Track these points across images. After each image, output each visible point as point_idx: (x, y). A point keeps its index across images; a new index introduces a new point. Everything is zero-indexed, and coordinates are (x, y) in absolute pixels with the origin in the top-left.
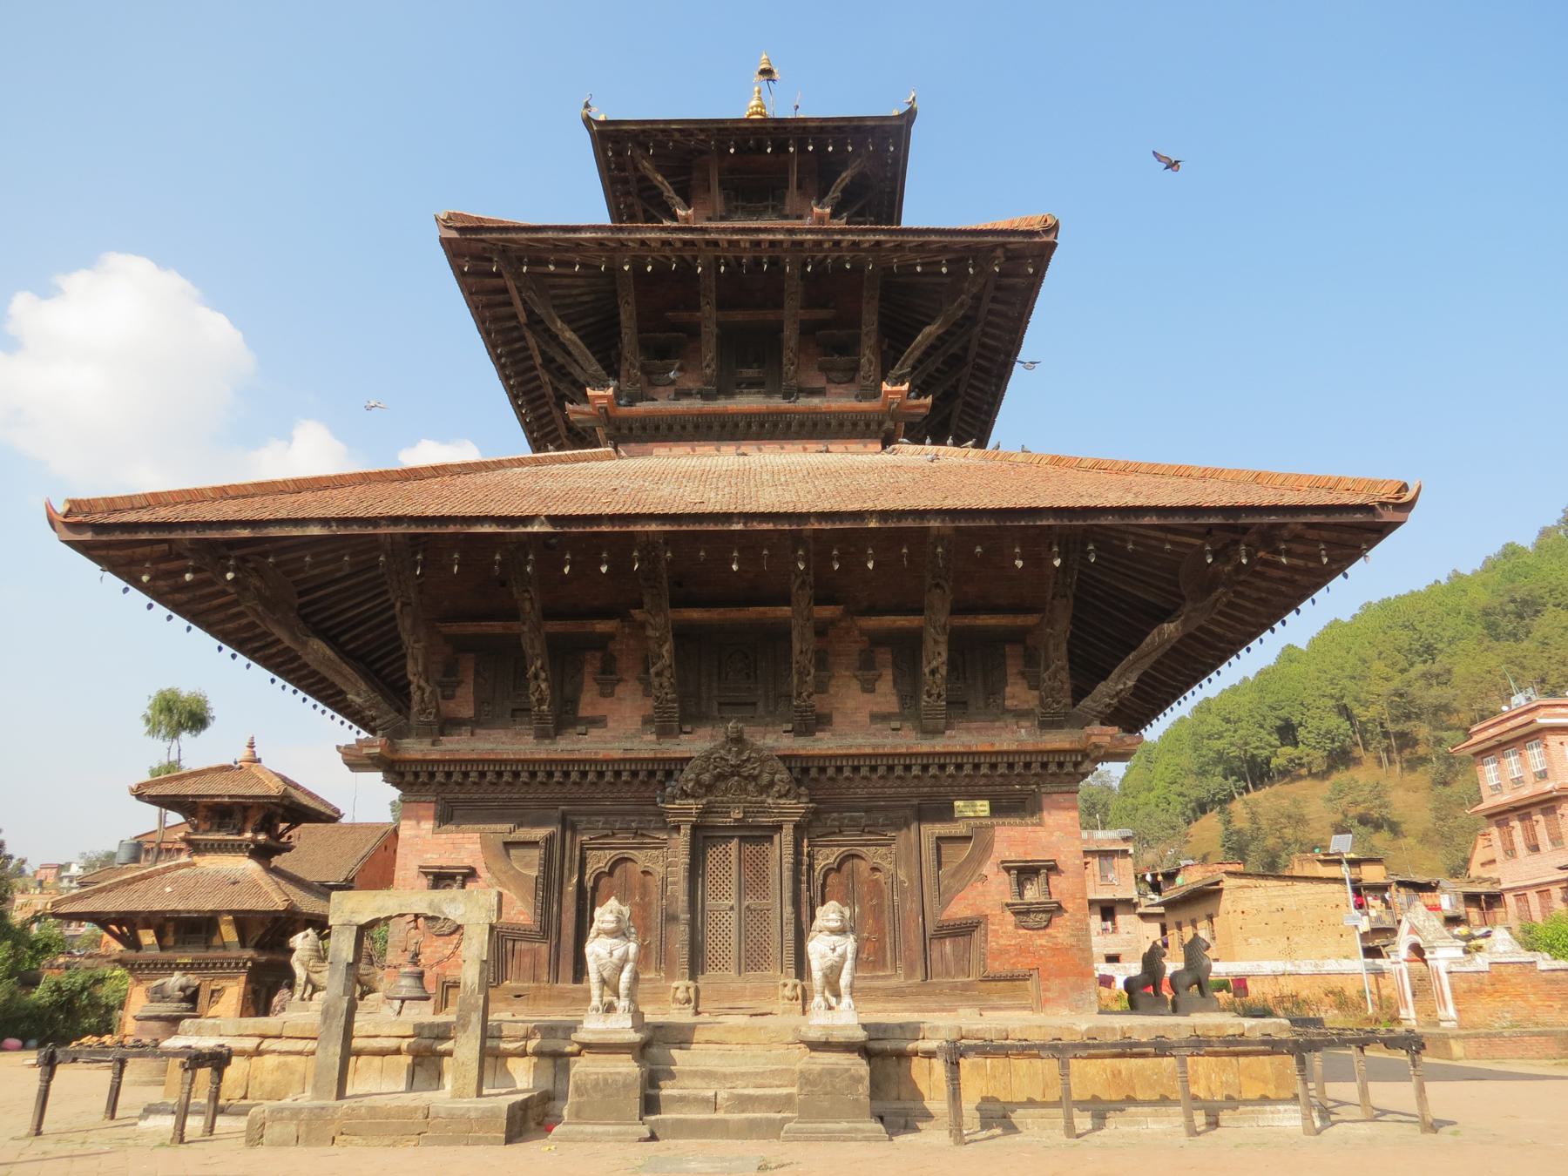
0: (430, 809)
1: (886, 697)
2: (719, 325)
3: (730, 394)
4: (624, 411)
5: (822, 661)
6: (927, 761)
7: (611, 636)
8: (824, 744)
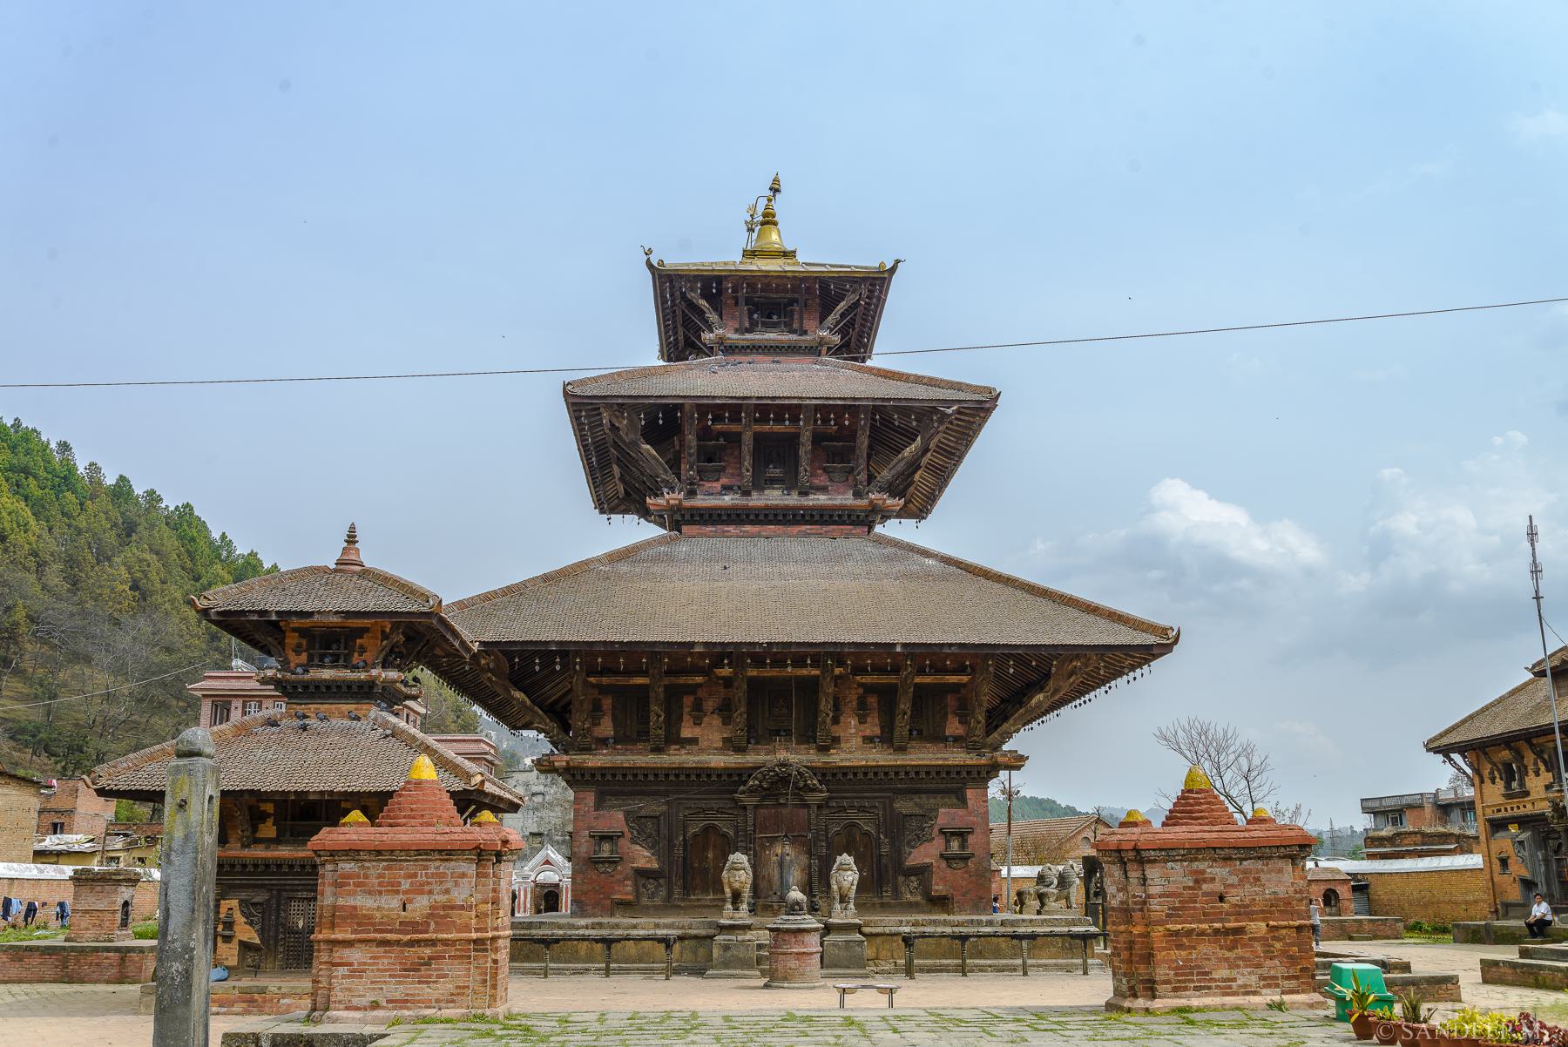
0: (590, 798)
1: (872, 728)
2: (759, 438)
3: (761, 489)
4: (687, 503)
5: (837, 708)
6: (897, 770)
7: (700, 685)
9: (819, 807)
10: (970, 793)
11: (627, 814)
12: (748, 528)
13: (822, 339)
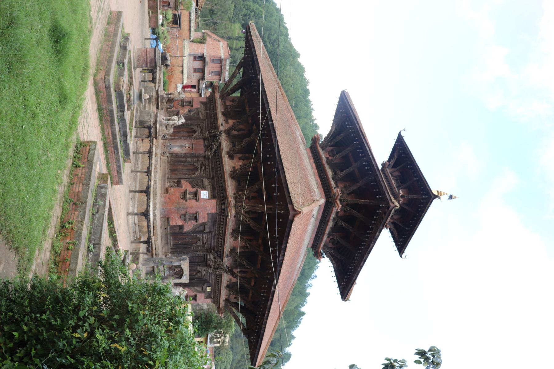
0: (205, 100)
8: (226, 159)
9: (205, 157)
10: (214, 201)
11: (200, 109)
12: (314, 165)
13: (399, 193)
